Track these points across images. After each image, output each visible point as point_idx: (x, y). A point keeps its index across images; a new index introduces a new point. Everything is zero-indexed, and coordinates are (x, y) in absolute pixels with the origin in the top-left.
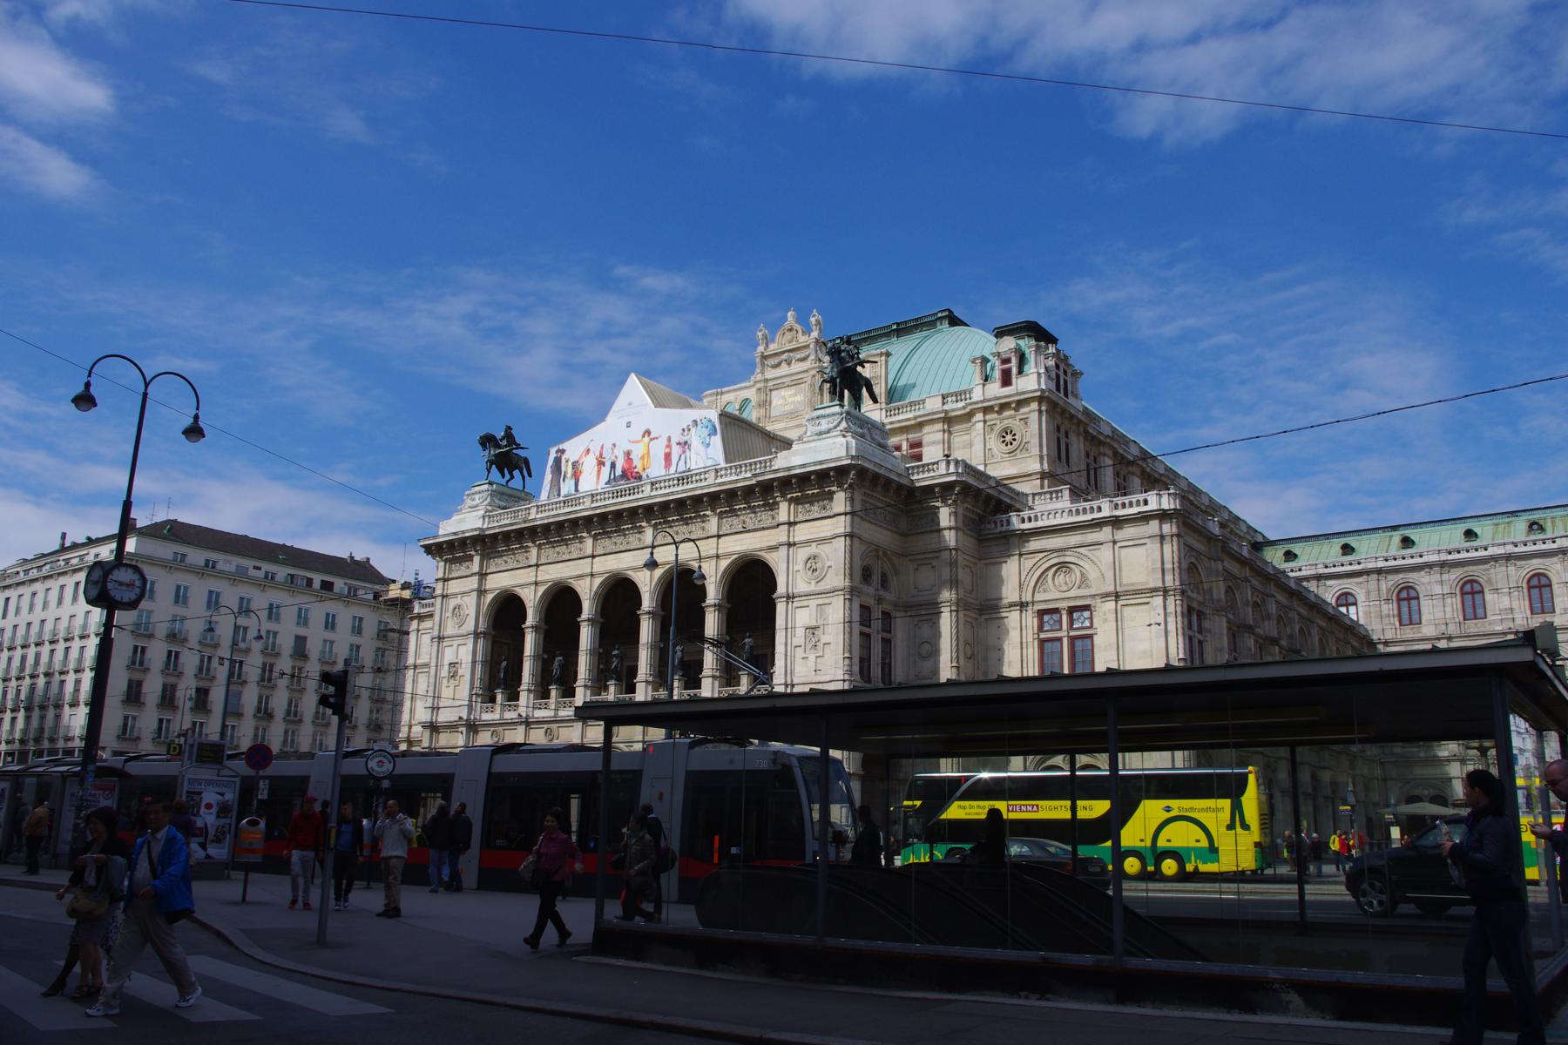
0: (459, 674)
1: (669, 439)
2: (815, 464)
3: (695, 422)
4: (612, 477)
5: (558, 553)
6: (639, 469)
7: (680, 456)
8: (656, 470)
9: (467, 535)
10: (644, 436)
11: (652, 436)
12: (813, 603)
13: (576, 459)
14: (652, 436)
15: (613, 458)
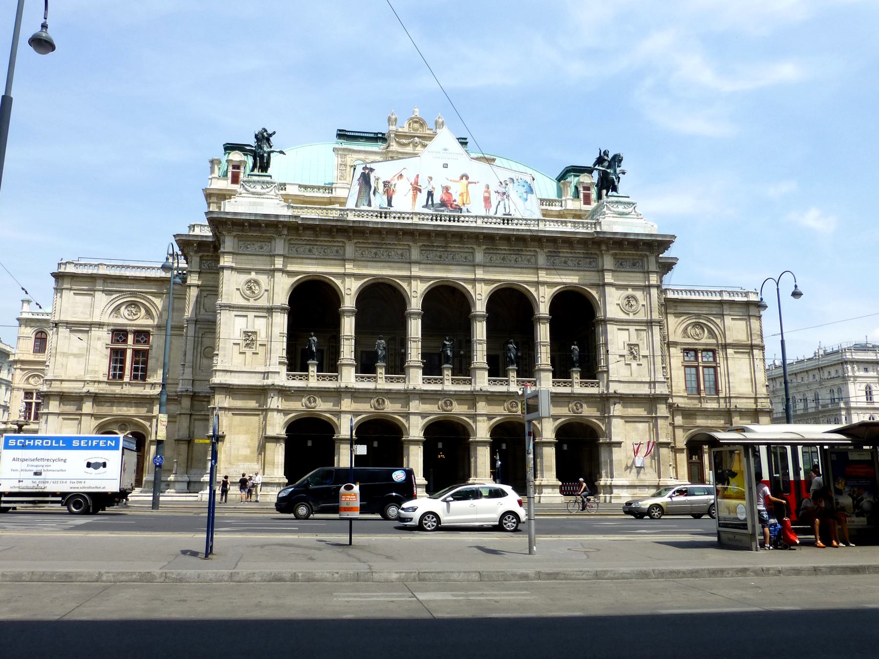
0: (258, 343)
1: (488, 187)
2: (647, 235)
3: (512, 180)
4: (430, 202)
5: (376, 254)
6: (459, 202)
7: (500, 202)
8: (476, 207)
9: (281, 219)
10: (462, 178)
11: (469, 180)
12: (632, 328)
13: (388, 179)
14: (469, 180)
15: (430, 188)
